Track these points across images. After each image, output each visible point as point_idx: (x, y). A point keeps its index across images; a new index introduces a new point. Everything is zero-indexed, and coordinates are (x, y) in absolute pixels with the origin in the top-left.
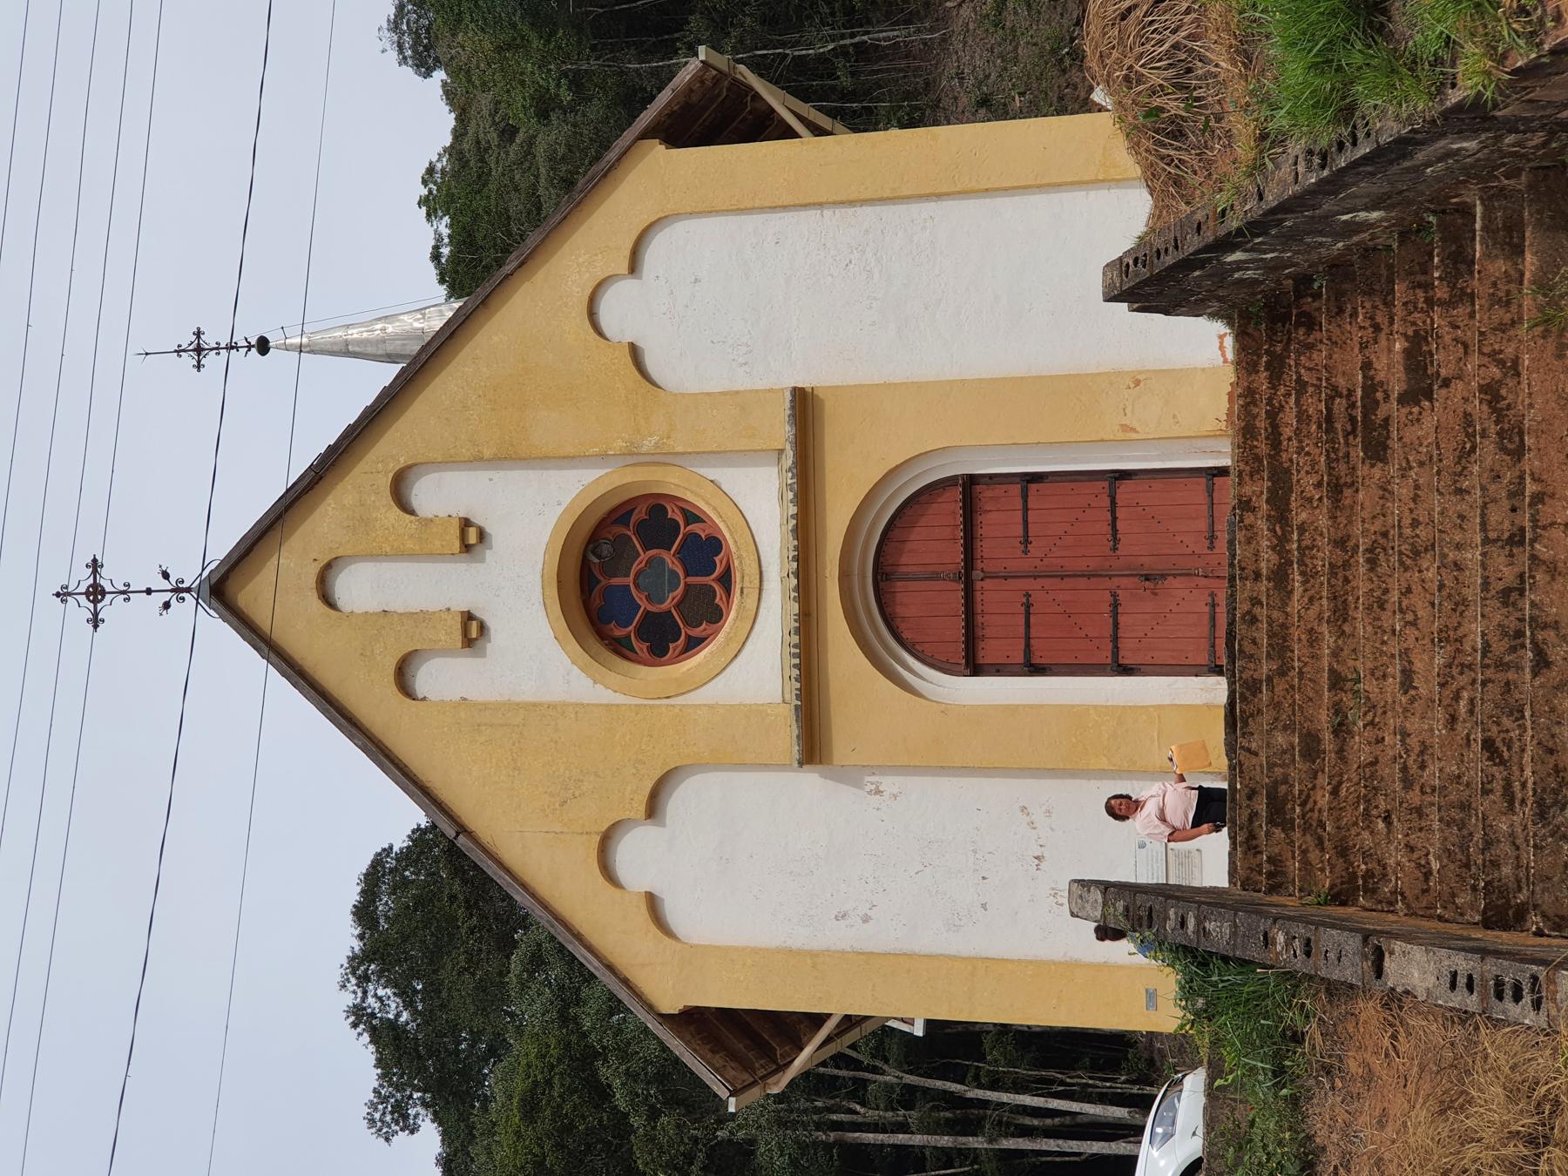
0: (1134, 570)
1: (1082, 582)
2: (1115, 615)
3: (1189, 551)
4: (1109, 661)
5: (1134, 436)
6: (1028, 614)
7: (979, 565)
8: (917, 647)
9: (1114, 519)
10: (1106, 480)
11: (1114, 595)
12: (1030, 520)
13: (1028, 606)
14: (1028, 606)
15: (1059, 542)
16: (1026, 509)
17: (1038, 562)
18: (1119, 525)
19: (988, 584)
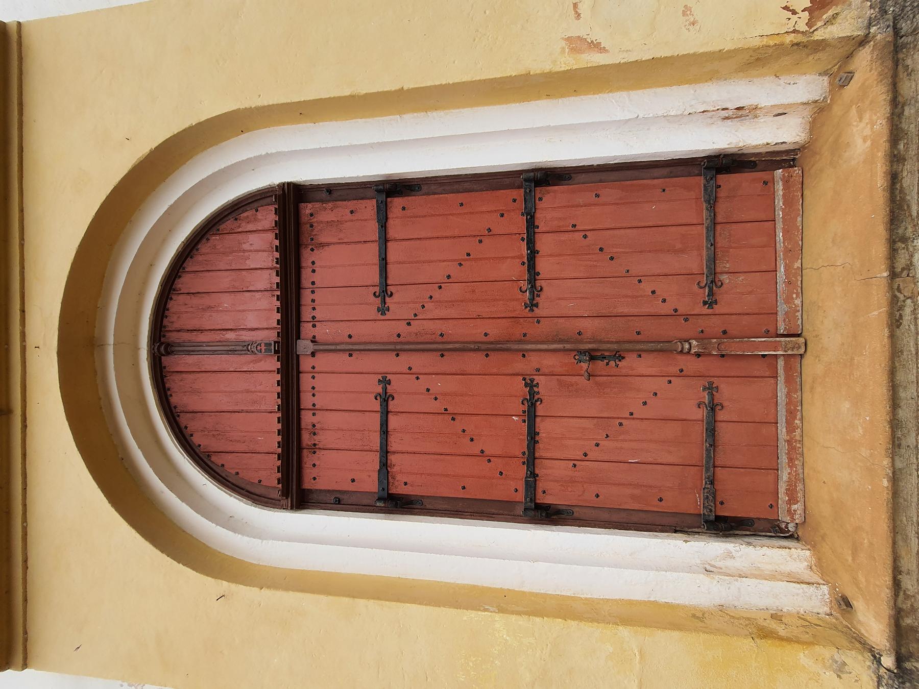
0: (567, 342)
1: (475, 362)
2: (531, 416)
3: (667, 309)
4: (520, 496)
5: (597, 59)
6: (385, 413)
7: (307, 330)
8: (213, 458)
9: (533, 254)
10: (520, 187)
11: (531, 385)
12: (391, 257)
13: (385, 399)
14: (385, 399)
15: (437, 295)
16: (384, 240)
17: (402, 327)
18: (543, 265)
19: (323, 362)
